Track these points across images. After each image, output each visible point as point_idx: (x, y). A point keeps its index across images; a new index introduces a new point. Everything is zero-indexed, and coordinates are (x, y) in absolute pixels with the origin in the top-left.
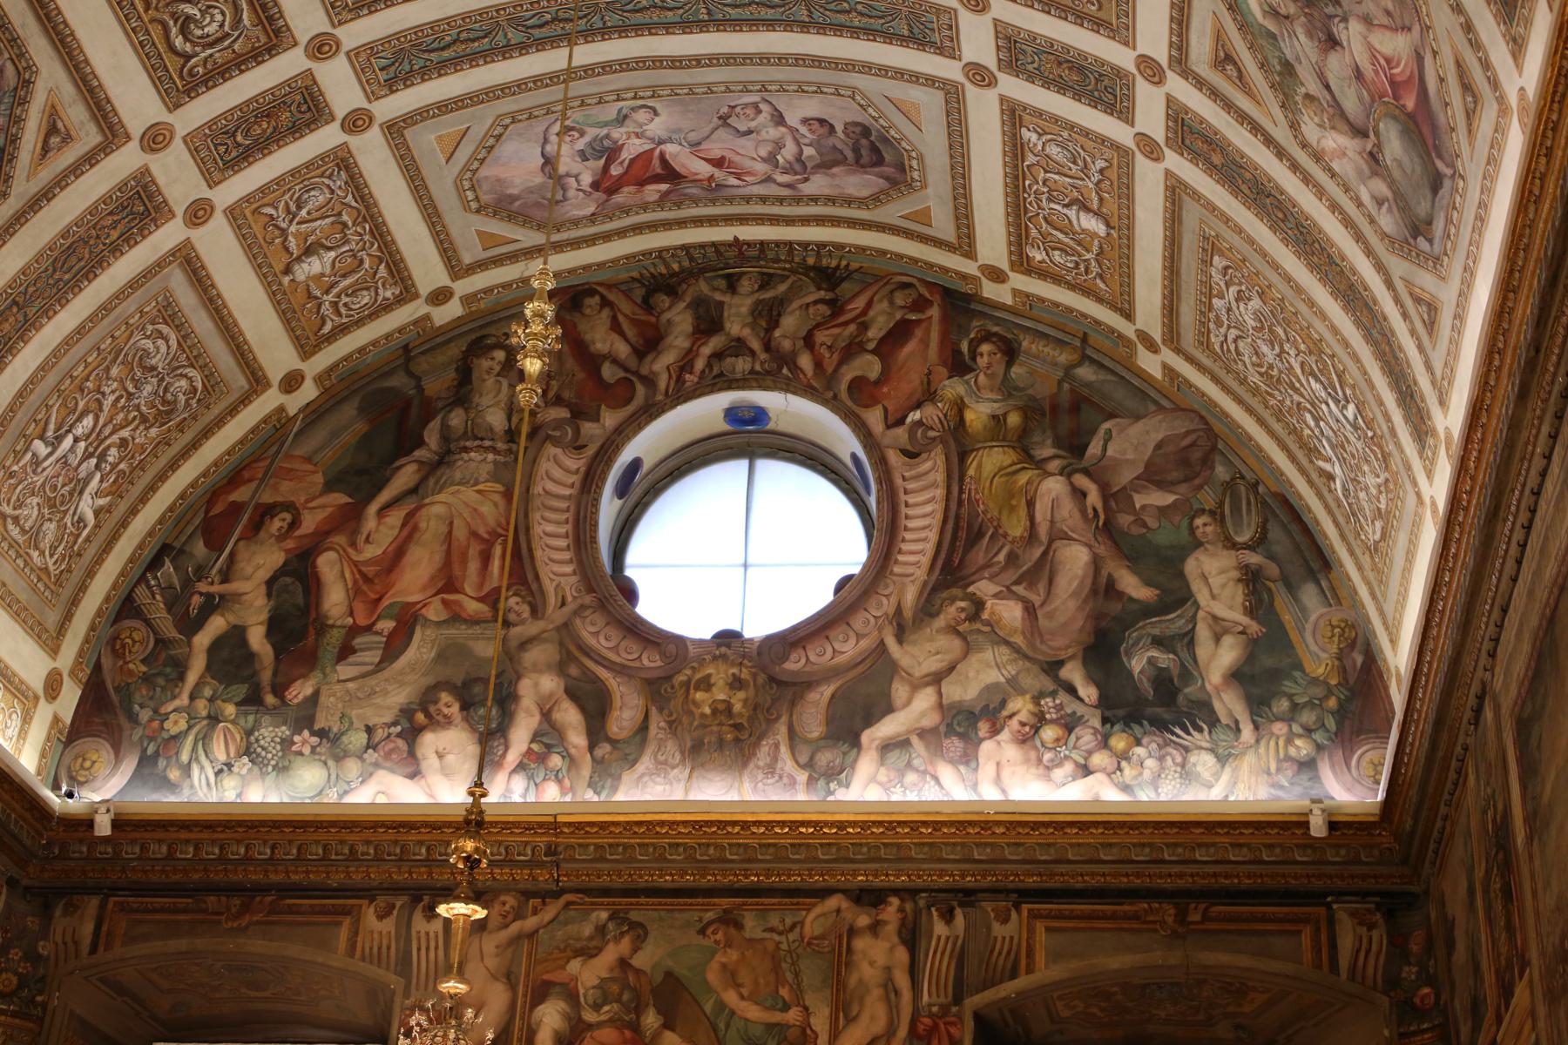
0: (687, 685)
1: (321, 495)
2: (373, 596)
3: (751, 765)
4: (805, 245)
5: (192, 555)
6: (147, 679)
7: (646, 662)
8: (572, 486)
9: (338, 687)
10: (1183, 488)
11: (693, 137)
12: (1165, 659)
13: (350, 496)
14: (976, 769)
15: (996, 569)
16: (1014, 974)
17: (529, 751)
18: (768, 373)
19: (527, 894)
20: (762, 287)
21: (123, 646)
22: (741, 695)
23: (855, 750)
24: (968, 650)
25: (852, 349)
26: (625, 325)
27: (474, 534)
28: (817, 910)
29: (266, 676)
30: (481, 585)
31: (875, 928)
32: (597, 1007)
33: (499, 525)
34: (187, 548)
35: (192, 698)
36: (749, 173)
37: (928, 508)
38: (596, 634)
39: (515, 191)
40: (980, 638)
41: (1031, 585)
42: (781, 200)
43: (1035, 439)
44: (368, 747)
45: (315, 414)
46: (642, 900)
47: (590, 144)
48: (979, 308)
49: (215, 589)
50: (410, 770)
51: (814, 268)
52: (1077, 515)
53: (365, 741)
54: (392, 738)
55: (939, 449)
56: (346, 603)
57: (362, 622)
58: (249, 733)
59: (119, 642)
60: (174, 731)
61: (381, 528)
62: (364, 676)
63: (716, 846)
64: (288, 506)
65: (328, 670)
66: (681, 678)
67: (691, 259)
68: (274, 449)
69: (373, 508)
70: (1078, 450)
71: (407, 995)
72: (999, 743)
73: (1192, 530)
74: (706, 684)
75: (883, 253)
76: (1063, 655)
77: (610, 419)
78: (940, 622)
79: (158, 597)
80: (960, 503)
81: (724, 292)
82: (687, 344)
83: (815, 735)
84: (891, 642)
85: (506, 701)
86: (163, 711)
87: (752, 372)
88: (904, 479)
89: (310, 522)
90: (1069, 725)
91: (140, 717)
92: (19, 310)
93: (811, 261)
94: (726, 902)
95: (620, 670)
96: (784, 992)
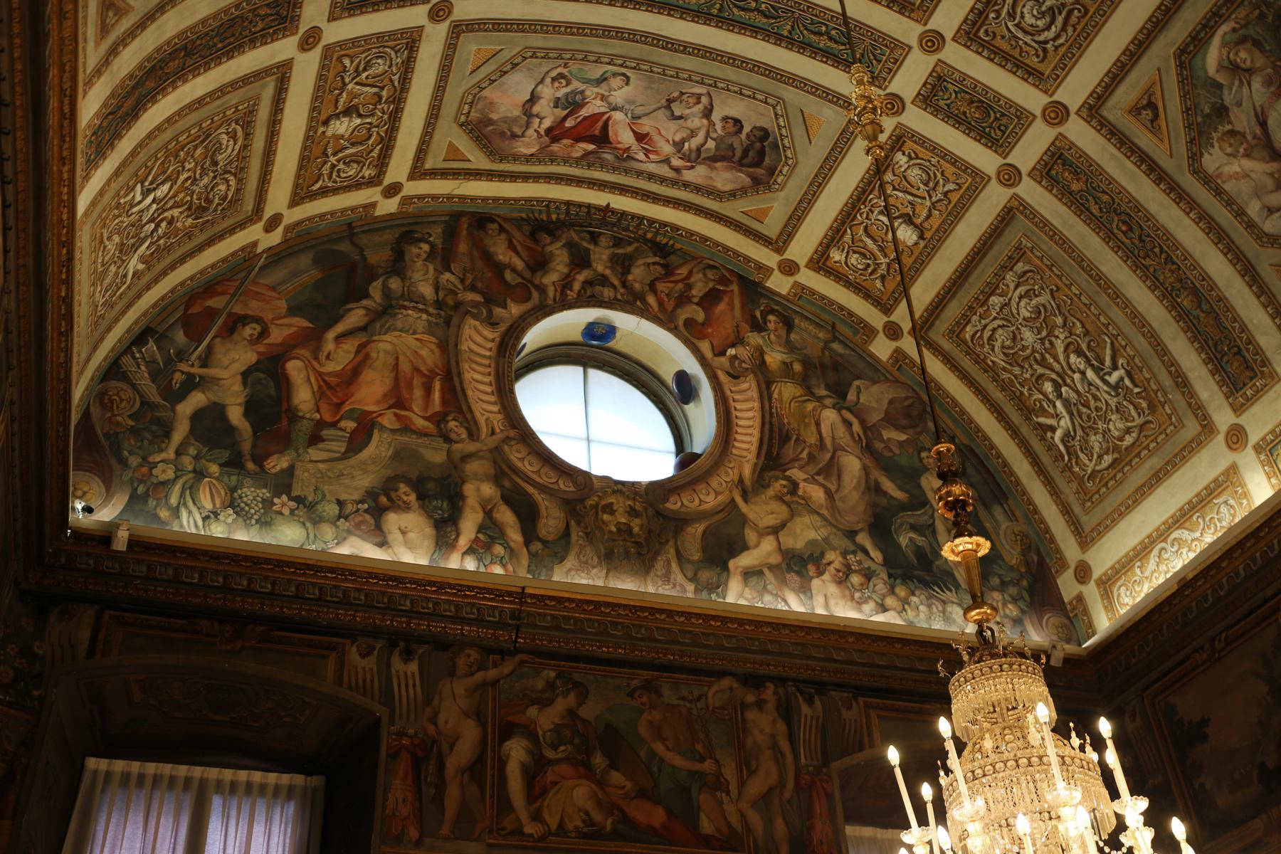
0: (596, 506)
1: (285, 317)
2: (336, 400)
3: (652, 574)
4: (652, 221)
6: (134, 432)
7: (562, 486)
8: (490, 350)
9: (311, 466)
10: (910, 431)
11: (639, 111)
12: (920, 540)
13: (311, 322)
14: (811, 598)
15: (802, 463)
16: (861, 749)
17: (476, 540)
18: (627, 302)
19: (487, 650)
20: (615, 245)
21: (112, 401)
22: (638, 521)
23: (726, 573)
24: (793, 514)
25: (683, 300)
26: (519, 248)
27: (417, 370)
28: (715, 688)
29: (246, 447)
30: (426, 408)
31: (760, 704)
32: (554, 747)
33: (437, 367)
35: (178, 453)
36: (656, 152)
37: (750, 414)
38: (522, 459)
39: (494, 116)
40: (800, 507)
41: (827, 477)
42: (663, 180)
43: (813, 382)
44: (340, 517)
45: (277, 256)
46: (581, 665)
47: (567, 95)
48: (764, 292)
49: (195, 370)
50: (379, 540)
51: (650, 241)
52: (849, 437)
53: (337, 512)
54: (361, 512)
55: (751, 377)
56: (313, 402)
57: (328, 418)
58: (233, 490)
59: (107, 397)
60: (163, 478)
61: (339, 350)
62: (332, 460)
63: (647, 628)
64: (257, 320)
65: (301, 451)
66: (590, 502)
67: (568, 214)
68: (243, 274)
69: (331, 335)
70: (843, 395)
71: (392, 722)
72: (823, 581)
73: (921, 460)
74: (610, 509)
75: (705, 239)
76: (856, 528)
77: (515, 310)
78: (771, 492)
79: (143, 368)
80: (771, 414)
81: (590, 243)
82: (566, 270)
83: (696, 558)
84: (739, 500)
85: (455, 502)
86: (151, 459)
87: (615, 299)
88: (731, 391)
89: (277, 335)
90: (868, 575)
91: (129, 462)
92: (185, 56)
93: (649, 236)
94: (646, 674)
95: (543, 489)
96: (699, 747)
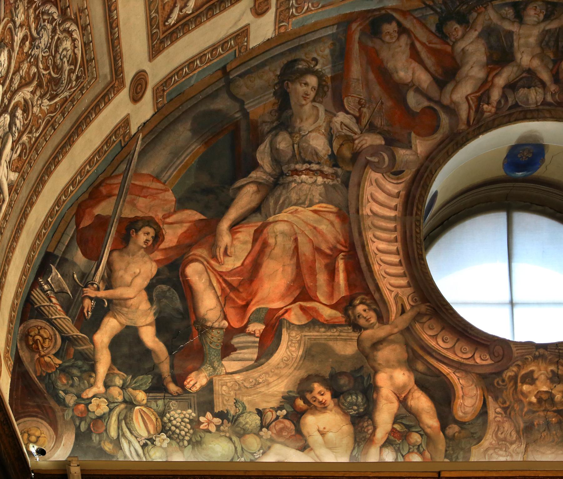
0: (514, 379)
1: (175, 212)
2: (241, 303)
5: (74, 264)
6: (63, 370)
7: (478, 361)
9: (227, 378)
13: (202, 213)
21: (36, 342)
27: (317, 250)
29: (165, 368)
30: (331, 295)
34: (68, 256)
35: (107, 385)
44: (262, 427)
49: (102, 294)
53: (259, 422)
56: (219, 308)
57: (236, 325)
58: (162, 415)
59: (30, 338)
60: (99, 412)
61: (235, 242)
62: (247, 369)
64: (150, 222)
65: (216, 364)
69: (225, 225)
79: (54, 300)
86: (85, 396)
91: (67, 401)
95: (458, 366)
